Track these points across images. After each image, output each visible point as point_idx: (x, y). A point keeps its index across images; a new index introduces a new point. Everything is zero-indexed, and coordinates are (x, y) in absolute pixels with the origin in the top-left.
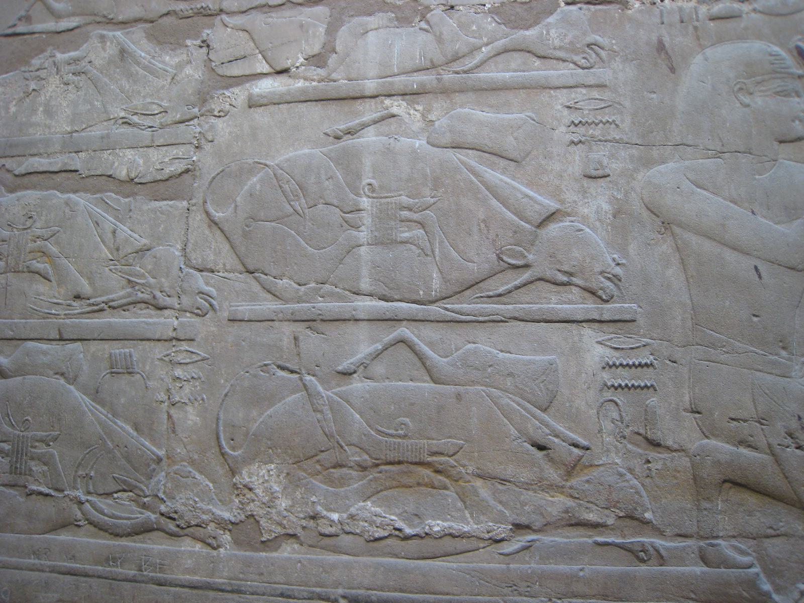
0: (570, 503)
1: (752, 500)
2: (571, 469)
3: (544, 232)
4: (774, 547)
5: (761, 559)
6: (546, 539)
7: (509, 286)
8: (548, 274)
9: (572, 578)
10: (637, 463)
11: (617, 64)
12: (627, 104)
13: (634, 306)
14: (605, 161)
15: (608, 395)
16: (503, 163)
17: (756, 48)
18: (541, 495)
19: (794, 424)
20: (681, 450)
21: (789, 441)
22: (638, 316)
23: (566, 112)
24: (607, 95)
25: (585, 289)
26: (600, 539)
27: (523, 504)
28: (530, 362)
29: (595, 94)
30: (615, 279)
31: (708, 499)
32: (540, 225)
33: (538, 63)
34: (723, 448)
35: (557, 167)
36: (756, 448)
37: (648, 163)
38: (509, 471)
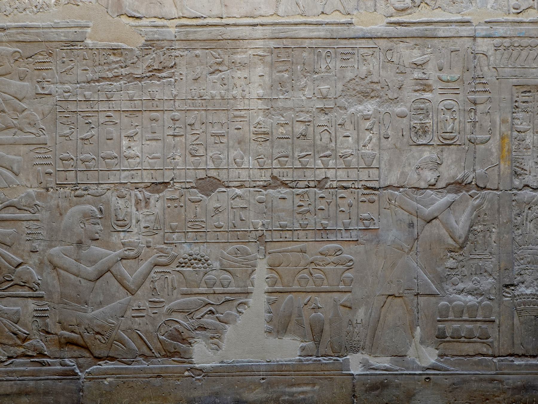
0: (24, 350)
1: (75, 348)
2: (25, 340)
3: (18, 269)
4: (81, 360)
5: (77, 364)
6: (17, 360)
7: (6, 287)
8: (18, 283)
9: (24, 371)
10: (43, 338)
11: (44, 212)
12: (45, 227)
13: (43, 292)
14: (37, 246)
15: (35, 319)
16: (5, 246)
17: (88, 207)
18: (16, 348)
19: (87, 327)
20: (56, 334)
21: (86, 331)
22: (44, 296)
23: (26, 229)
24: (38, 223)
25: (29, 287)
26: (32, 360)
27: (10, 351)
28: (13, 310)
29: (36, 223)
30: (38, 284)
31: (63, 348)
32: (17, 267)
33: (18, 211)
34: (67, 333)
35: (22, 248)
36: (76, 333)
37: (51, 247)
38: (6, 341)
